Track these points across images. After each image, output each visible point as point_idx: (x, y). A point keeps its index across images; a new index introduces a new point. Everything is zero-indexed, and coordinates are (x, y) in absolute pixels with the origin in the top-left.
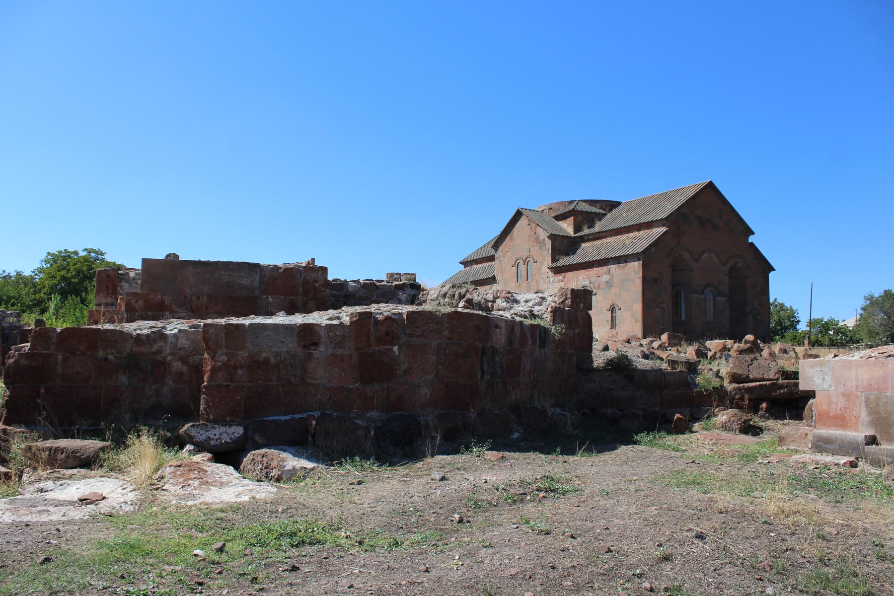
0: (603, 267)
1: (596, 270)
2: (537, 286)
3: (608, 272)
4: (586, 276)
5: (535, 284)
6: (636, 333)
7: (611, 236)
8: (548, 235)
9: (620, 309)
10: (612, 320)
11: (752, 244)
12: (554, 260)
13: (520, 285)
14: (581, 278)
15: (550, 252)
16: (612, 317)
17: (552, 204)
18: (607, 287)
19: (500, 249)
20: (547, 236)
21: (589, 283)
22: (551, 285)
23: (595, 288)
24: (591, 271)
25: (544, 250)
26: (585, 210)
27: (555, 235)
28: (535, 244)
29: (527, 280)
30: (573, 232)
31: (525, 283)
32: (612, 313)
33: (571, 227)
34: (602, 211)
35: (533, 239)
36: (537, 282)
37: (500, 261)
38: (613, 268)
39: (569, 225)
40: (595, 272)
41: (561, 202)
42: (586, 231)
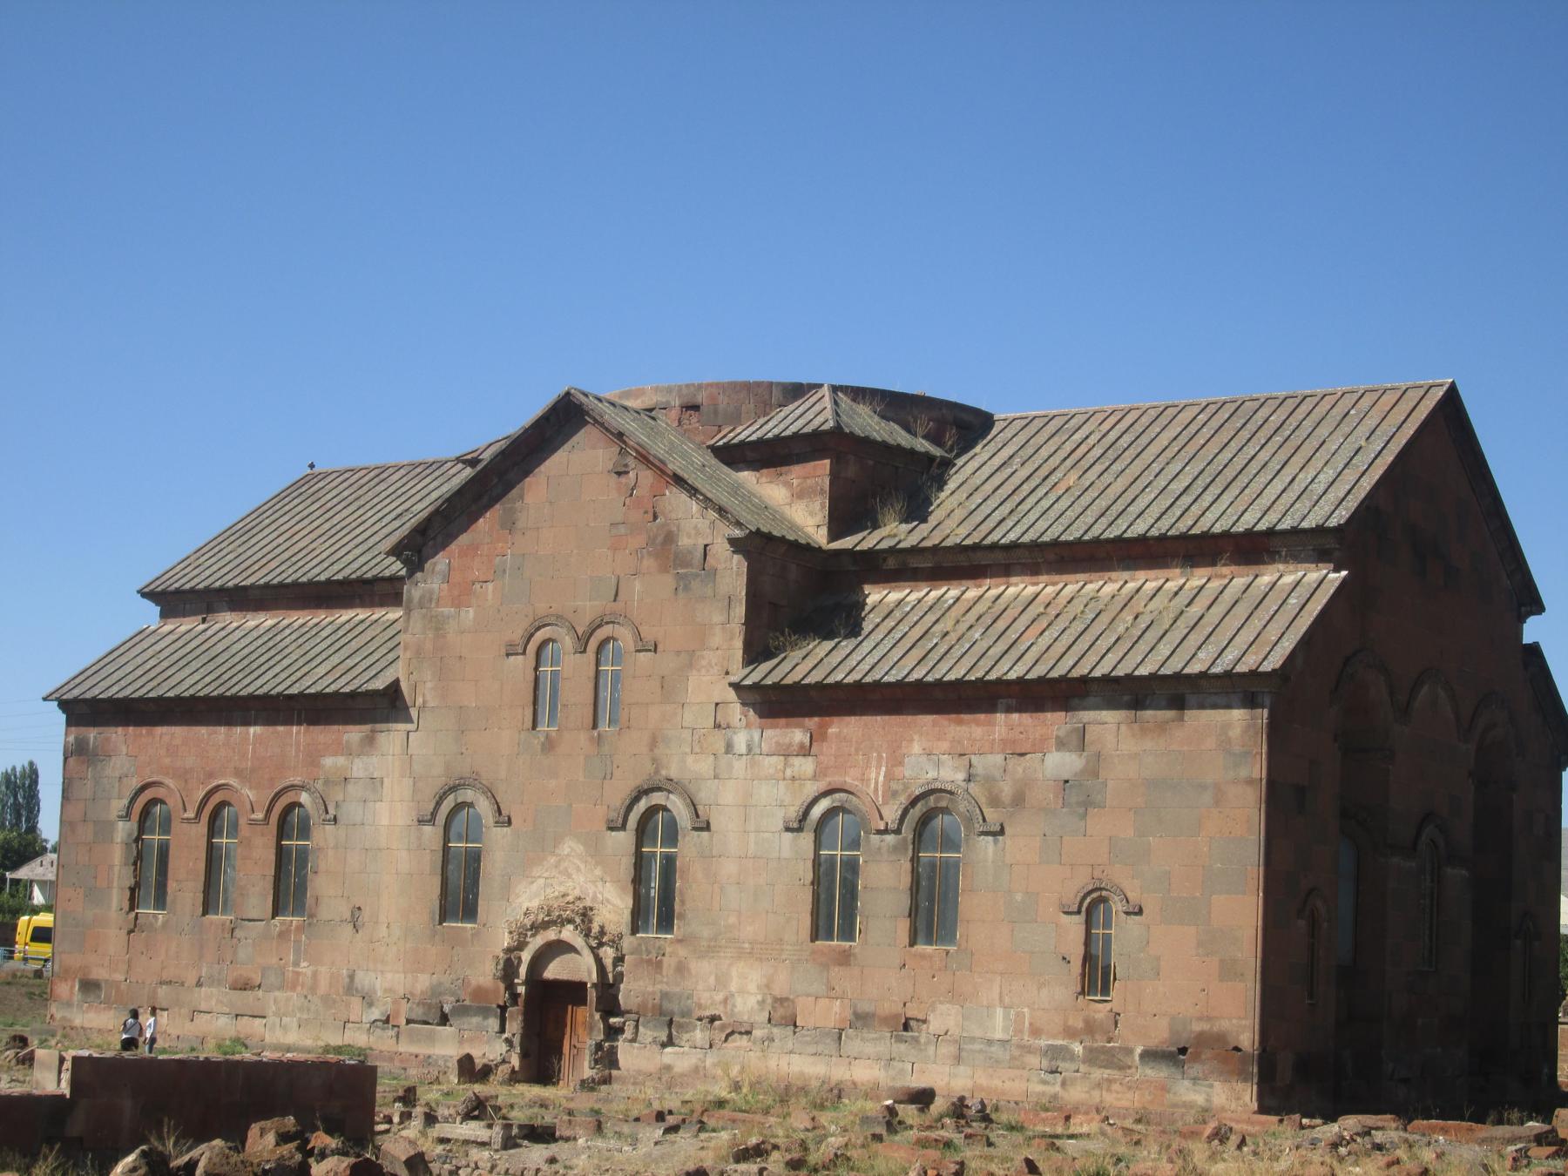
0: (1049, 716)
1: (1003, 724)
2: (654, 760)
4: (945, 745)
6: (1224, 1025)
7: (1033, 570)
8: (738, 533)
9: (1140, 912)
10: (1088, 958)
11: (1535, 650)
12: (756, 651)
13: (549, 745)
14: (916, 748)
15: (740, 611)
16: (1088, 942)
17: (700, 387)
19: (440, 562)
20: (733, 541)
21: (960, 776)
22: (739, 766)
23: (995, 802)
24: (978, 723)
26: (880, 439)
27: (769, 537)
28: (649, 563)
29: (595, 726)
30: (824, 531)
31: (583, 738)
32: (1089, 924)
33: (817, 505)
34: (936, 451)
35: (639, 541)
36: (653, 743)
37: (438, 626)
38: (1106, 723)
39: (799, 495)
41: (748, 387)
42: (892, 533)
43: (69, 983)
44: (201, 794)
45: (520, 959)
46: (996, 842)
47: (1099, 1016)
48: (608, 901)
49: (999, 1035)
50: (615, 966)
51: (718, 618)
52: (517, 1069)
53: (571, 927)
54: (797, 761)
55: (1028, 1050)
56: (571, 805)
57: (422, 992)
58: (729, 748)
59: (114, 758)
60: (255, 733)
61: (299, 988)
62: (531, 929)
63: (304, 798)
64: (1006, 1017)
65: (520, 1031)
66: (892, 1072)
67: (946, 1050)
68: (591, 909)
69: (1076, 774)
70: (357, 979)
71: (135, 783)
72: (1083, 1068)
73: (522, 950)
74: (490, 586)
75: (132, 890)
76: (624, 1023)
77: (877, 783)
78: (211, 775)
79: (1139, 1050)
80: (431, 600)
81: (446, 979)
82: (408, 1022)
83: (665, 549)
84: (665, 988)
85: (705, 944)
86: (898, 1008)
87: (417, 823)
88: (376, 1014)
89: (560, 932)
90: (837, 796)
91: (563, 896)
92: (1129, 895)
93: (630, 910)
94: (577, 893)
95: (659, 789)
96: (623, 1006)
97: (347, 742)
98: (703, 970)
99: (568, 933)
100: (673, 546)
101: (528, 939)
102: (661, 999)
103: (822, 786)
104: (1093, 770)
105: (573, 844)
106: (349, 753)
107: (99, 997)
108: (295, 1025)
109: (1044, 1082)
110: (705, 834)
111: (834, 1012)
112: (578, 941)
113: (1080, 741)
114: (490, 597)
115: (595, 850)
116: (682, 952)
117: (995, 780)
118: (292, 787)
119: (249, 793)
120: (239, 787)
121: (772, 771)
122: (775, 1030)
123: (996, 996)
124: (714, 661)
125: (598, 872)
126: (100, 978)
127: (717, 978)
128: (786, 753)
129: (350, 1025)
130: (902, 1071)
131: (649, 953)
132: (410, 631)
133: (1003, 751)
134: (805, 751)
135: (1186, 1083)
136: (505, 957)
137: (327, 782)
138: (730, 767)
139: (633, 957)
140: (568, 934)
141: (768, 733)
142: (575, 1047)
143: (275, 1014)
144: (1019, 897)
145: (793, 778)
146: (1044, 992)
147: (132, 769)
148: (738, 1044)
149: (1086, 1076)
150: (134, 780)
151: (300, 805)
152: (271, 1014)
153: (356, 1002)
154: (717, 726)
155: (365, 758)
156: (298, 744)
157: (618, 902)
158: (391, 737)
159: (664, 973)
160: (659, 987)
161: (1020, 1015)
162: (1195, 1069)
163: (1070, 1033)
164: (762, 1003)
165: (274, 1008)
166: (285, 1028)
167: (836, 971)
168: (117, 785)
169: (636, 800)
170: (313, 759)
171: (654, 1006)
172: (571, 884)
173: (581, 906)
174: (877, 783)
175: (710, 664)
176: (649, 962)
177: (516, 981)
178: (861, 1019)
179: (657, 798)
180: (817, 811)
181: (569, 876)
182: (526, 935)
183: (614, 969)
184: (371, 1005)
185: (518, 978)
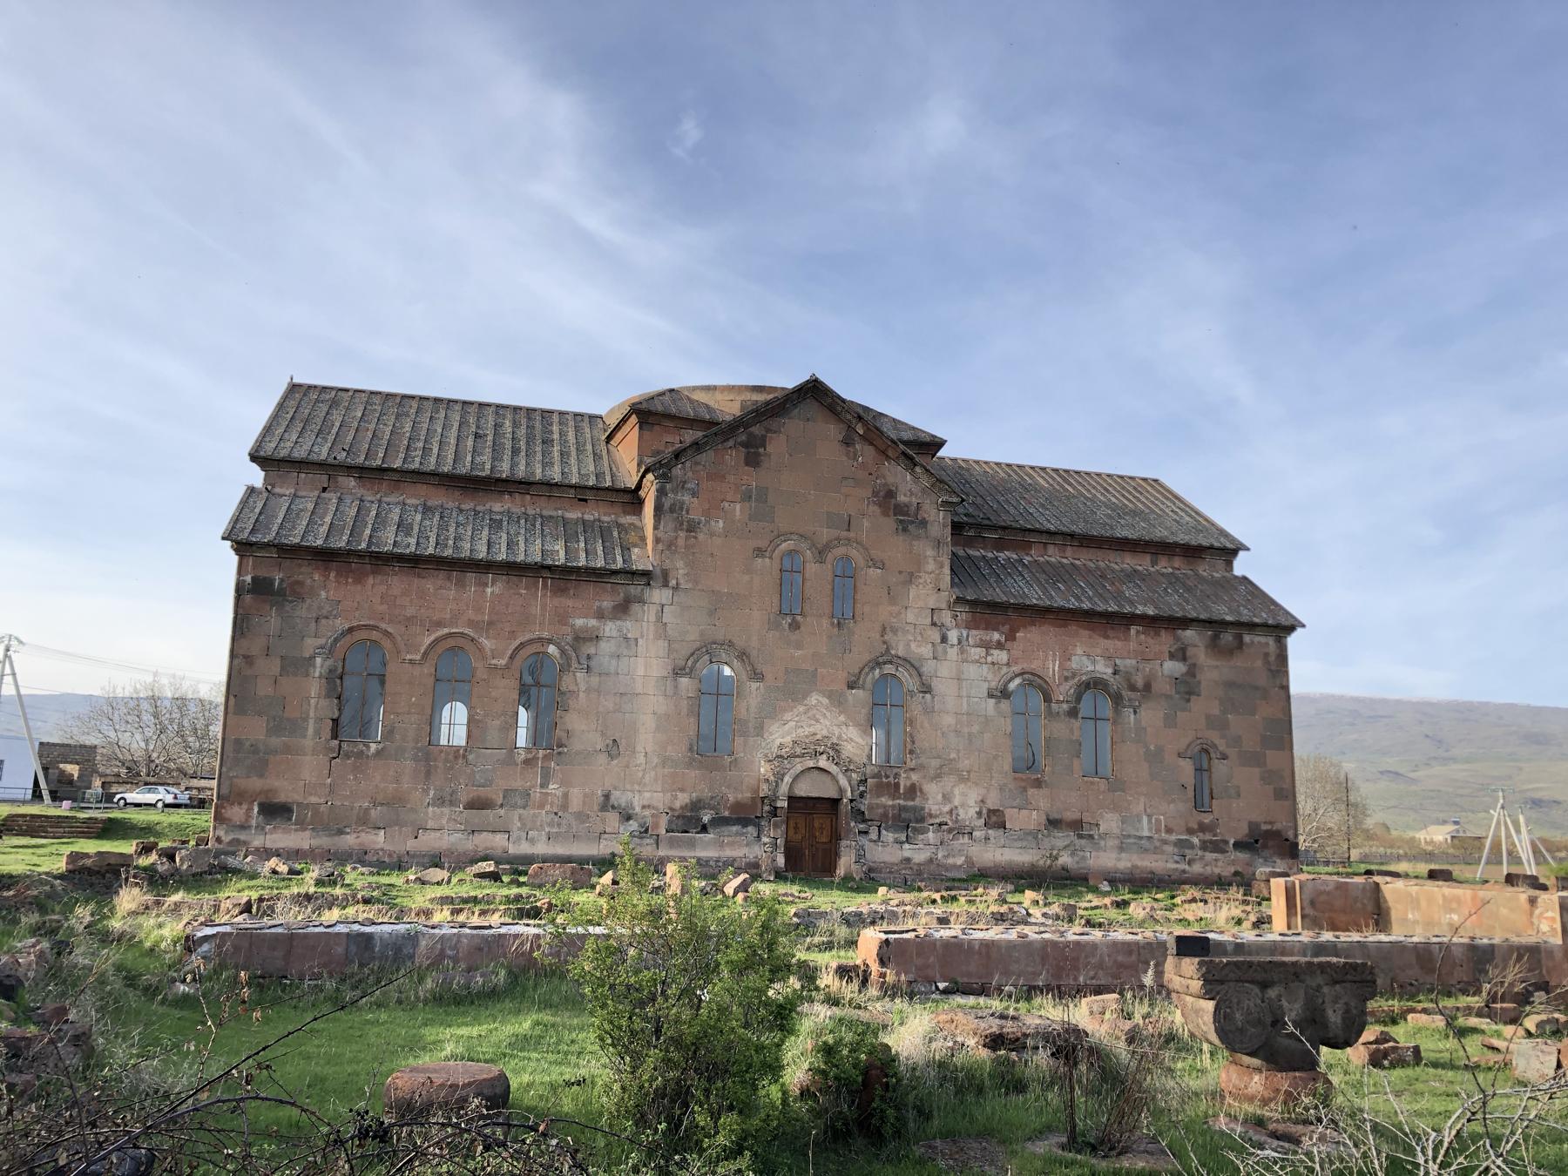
2: (885, 643)
3: (1180, 655)
4: (1099, 651)
5: (878, 636)
6: (1277, 826)
14: (1079, 651)
18: (1178, 693)
21: (1110, 671)
22: (953, 653)
23: (1132, 688)
24: (1119, 639)
25: (918, 537)
28: (877, 509)
31: (825, 622)
37: (692, 528)
40: (1132, 645)
43: (245, 806)
44: (428, 641)
46: (1135, 712)
47: (1206, 821)
48: (851, 739)
49: (1146, 833)
51: (930, 552)
53: (824, 756)
54: (996, 652)
55: (1165, 842)
56: (816, 669)
57: (682, 808)
58: (944, 639)
59: (309, 601)
60: (492, 593)
61: (548, 807)
63: (552, 649)
64: (1150, 821)
66: (1076, 859)
67: (1112, 843)
69: (1182, 675)
70: (613, 800)
71: (341, 624)
72: (1200, 853)
74: (738, 506)
75: (335, 721)
77: (1054, 671)
78: (439, 624)
79: (1232, 841)
80: (682, 509)
81: (707, 794)
82: (667, 831)
83: (886, 499)
84: (901, 802)
85: (932, 772)
86: (1076, 816)
87: (671, 674)
88: (634, 825)
90: (1026, 676)
92: (1221, 749)
94: (825, 733)
95: (891, 663)
96: (867, 817)
97: (599, 608)
98: (933, 791)
99: (825, 762)
100: (893, 501)
102: (900, 810)
103: (1016, 669)
104: (1192, 671)
105: (820, 699)
106: (600, 615)
107: (290, 819)
108: (544, 838)
109: (1177, 862)
110: (928, 696)
111: (1031, 819)
112: (833, 769)
113: (1180, 654)
114: (738, 513)
115: (837, 701)
116: (915, 777)
117: (1131, 674)
118: (540, 639)
119: (487, 644)
120: (476, 637)
121: (977, 657)
122: (990, 832)
123: (1143, 809)
124: (929, 581)
125: (842, 718)
126: (290, 800)
127: (944, 796)
128: (987, 646)
129: (606, 836)
130: (1084, 858)
131: (887, 777)
132: (661, 528)
133: (1135, 658)
134: (1000, 646)
135: (1260, 860)
137: (577, 639)
138: (945, 652)
139: (875, 780)
140: (823, 762)
141: (974, 632)
143: (519, 829)
144: (1152, 748)
145: (993, 663)
146: (1172, 805)
147: (335, 612)
148: (961, 841)
149: (1202, 858)
150: (338, 621)
151: (546, 654)
152: (515, 829)
153: (612, 818)
154: (934, 624)
155: (618, 623)
156: (544, 607)
157: (860, 740)
158: (646, 608)
159: (901, 791)
160: (898, 801)
161: (1157, 820)
162: (1266, 853)
163: (1190, 831)
164: (979, 814)
165: (519, 824)
166: (532, 841)
167: (1031, 791)
168: (314, 624)
169: (873, 669)
170: (563, 619)
171: (893, 815)
174: (1054, 671)
175: (925, 582)
176: (889, 784)
178: (1054, 823)
179: (889, 669)
180: (1012, 686)
181: (817, 721)
184: (629, 818)
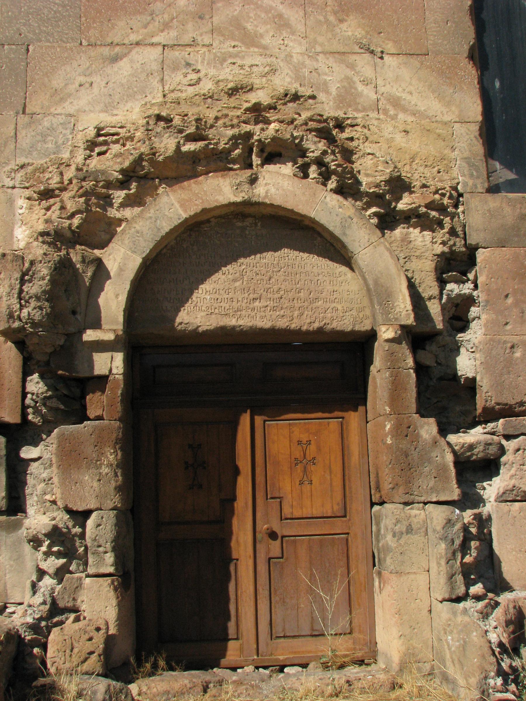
45: (99, 263)
50: (442, 283)
52: (112, 631)
62: (123, 184)
65: (115, 500)
68: (340, 126)
73: (103, 245)
76: (502, 451)
89: (253, 180)
91: (233, 92)
93: (475, 128)
101: (113, 213)
136: (56, 256)
142: (273, 535)
172: (258, 60)
173: (305, 115)
177: (90, 335)
182: (107, 201)
183: (442, 289)
185: (97, 325)
